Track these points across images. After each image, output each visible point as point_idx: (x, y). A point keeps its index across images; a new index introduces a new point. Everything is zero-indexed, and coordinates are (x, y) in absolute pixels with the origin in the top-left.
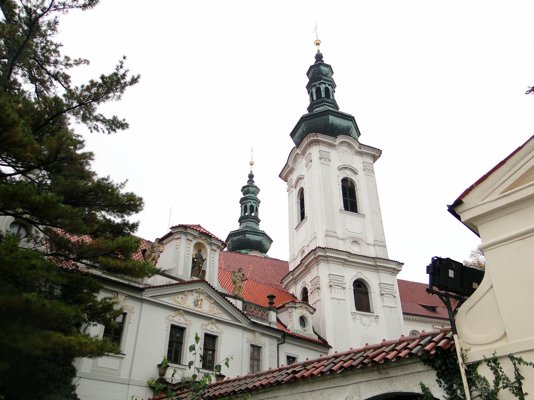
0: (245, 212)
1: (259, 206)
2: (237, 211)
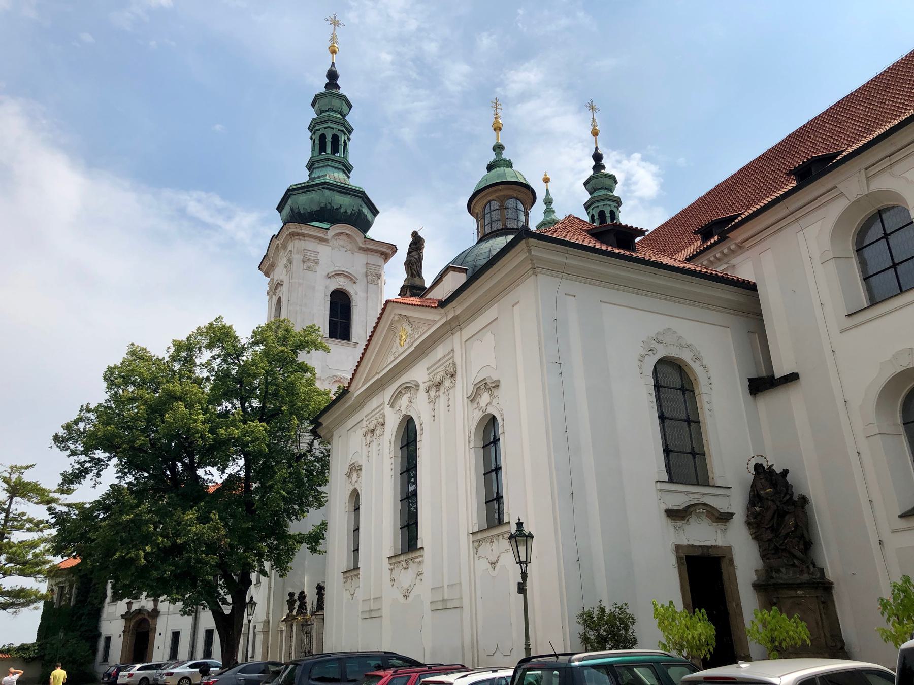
0: (322, 148)
2: (305, 149)
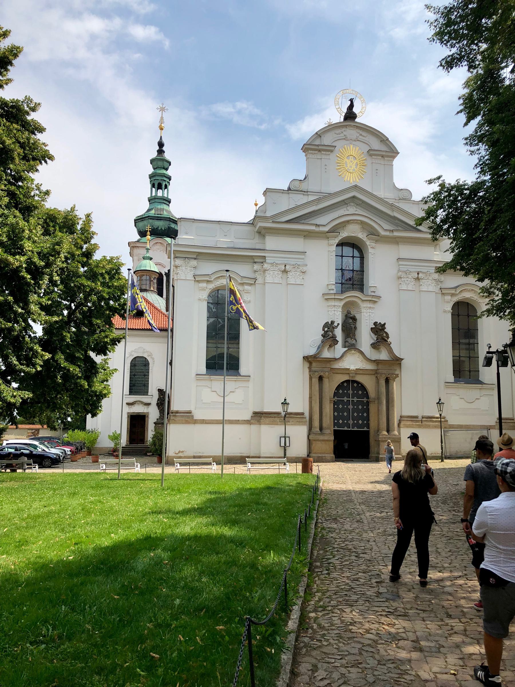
1: (169, 183)
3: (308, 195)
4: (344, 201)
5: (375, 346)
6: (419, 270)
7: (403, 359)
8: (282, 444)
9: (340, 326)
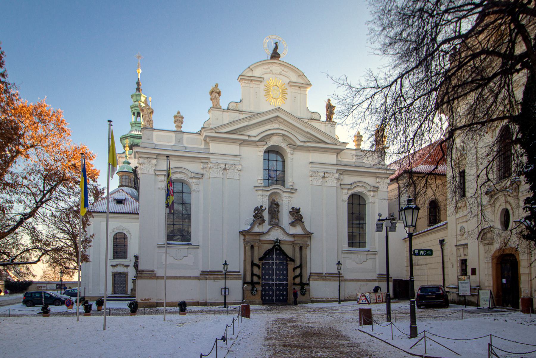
3: (242, 114)
4: (270, 119)
5: (292, 224)
6: (325, 170)
7: (312, 234)
8: (223, 293)
9: (267, 210)
